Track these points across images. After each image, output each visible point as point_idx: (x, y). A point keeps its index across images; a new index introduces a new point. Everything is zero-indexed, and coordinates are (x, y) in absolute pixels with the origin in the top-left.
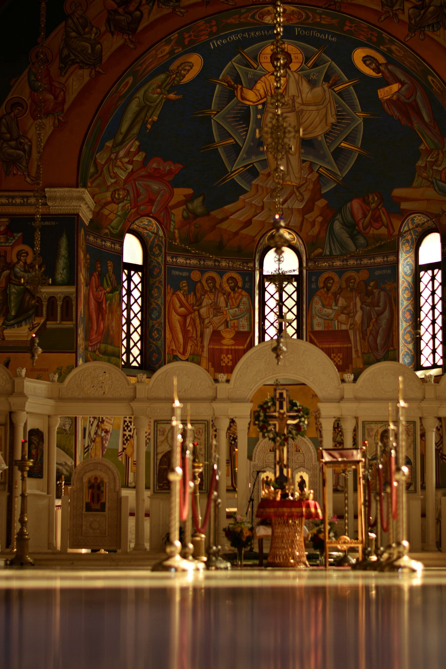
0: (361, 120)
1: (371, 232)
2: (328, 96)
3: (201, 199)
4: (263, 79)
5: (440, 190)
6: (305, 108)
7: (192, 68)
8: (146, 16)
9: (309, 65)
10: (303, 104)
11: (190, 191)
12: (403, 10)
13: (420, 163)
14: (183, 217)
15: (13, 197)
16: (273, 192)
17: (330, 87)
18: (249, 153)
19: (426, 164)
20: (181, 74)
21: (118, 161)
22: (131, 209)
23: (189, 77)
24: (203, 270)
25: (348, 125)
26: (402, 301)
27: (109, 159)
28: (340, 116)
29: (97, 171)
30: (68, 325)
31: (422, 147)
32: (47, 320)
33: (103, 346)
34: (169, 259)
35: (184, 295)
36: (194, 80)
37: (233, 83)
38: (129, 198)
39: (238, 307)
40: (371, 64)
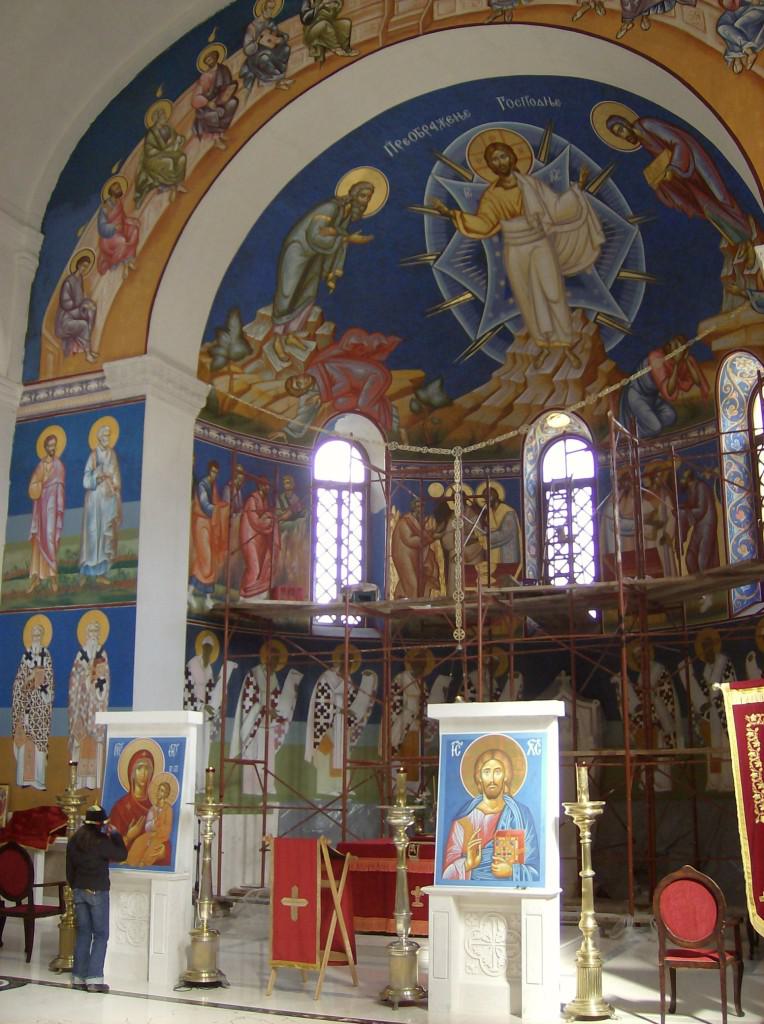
0: (636, 230)
1: (680, 397)
2: (583, 204)
4: (487, 195)
5: (759, 306)
6: (558, 229)
7: (373, 192)
8: (241, 103)
9: (542, 158)
13: (726, 272)
14: (412, 410)
15: (70, 386)
16: (536, 361)
17: (583, 188)
18: (497, 310)
19: (734, 271)
20: (358, 202)
21: (291, 336)
22: (322, 402)
23: (376, 203)
26: (730, 493)
28: (608, 230)
31: (723, 245)
37: (446, 209)
38: (316, 387)
40: (620, 130)
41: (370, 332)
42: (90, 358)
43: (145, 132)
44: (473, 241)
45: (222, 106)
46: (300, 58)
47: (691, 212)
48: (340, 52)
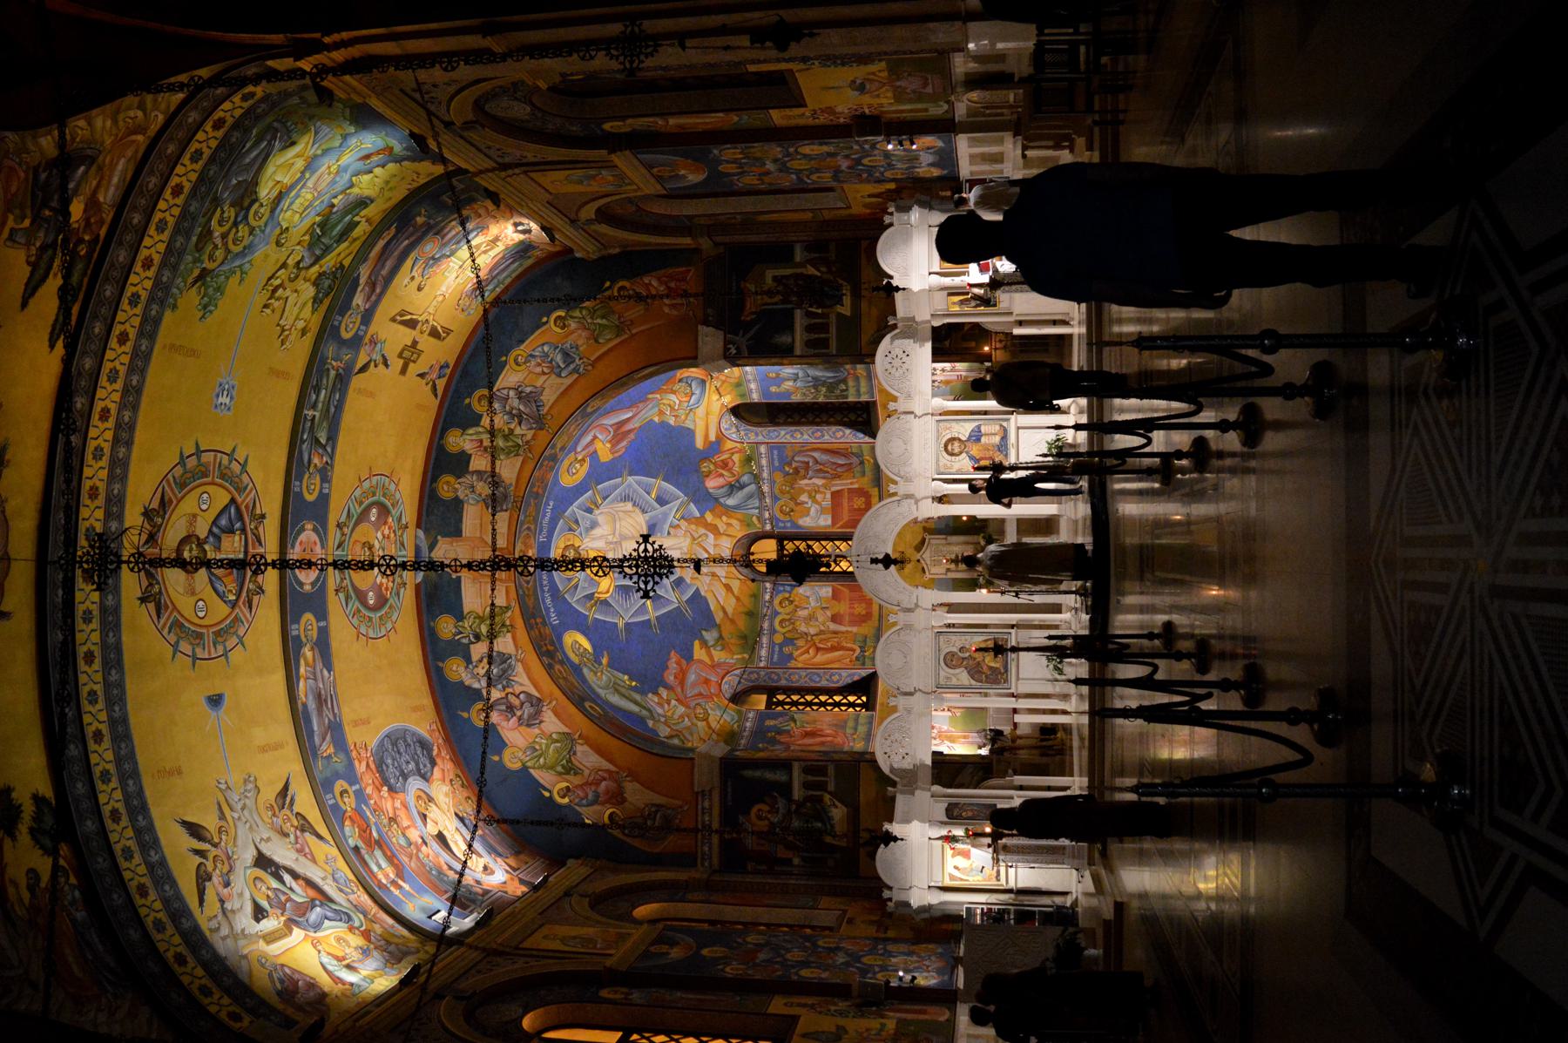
0: (630, 479)
3: (704, 633)
6: (617, 532)
10: (614, 534)
11: (697, 643)
12: (523, 435)
13: (672, 421)
23: (586, 644)
24: (773, 631)
25: (634, 491)
27: (665, 723)
28: (626, 498)
29: (677, 736)
30: (831, 770)
31: (656, 419)
32: (826, 791)
33: (849, 731)
34: (762, 665)
35: (797, 650)
36: (590, 640)
39: (808, 597)
41: (667, 667)
42: (685, 808)
43: (525, 769)
44: (615, 590)
45: (522, 704)
46: (504, 644)
47: (632, 436)
48: (509, 614)
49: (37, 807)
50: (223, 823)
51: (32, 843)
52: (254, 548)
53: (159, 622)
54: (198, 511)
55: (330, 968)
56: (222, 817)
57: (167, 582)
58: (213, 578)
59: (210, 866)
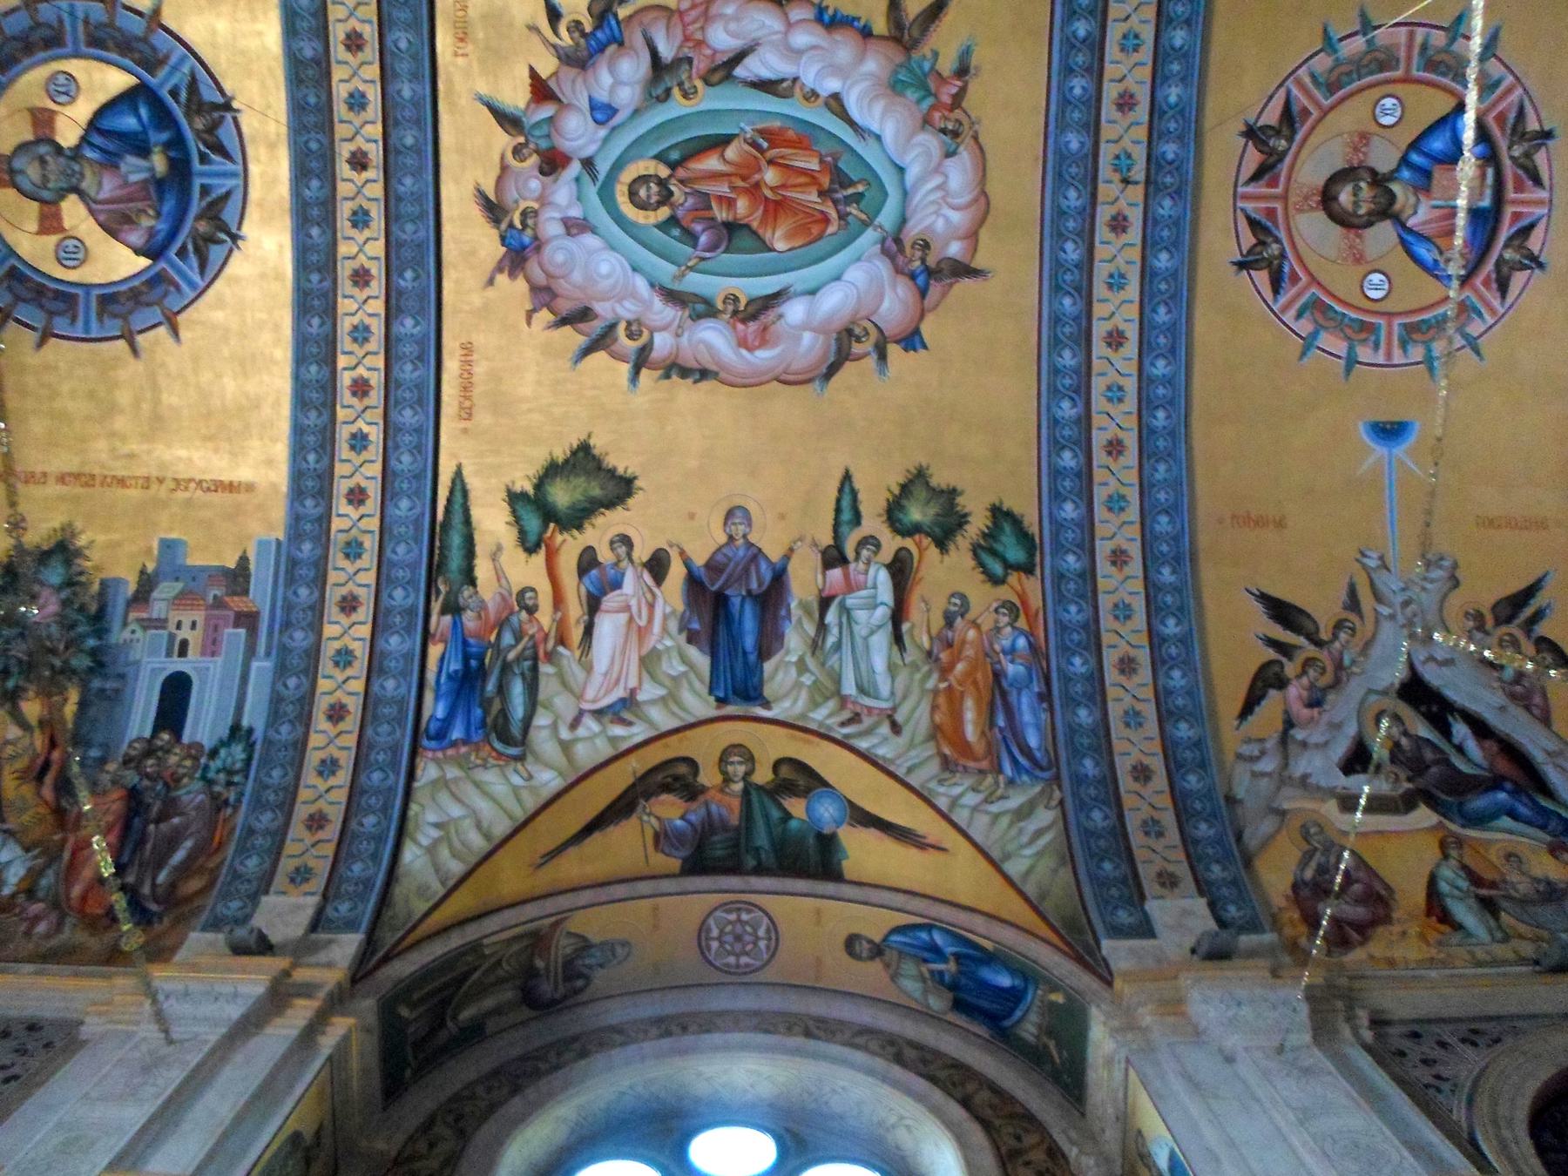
49: (995, 523)
50: (1353, 617)
51: (973, 563)
52: (1519, 188)
53: (1275, 300)
54: (1374, 128)
55: (1444, 887)
56: (1353, 603)
57: (1297, 239)
58: (1410, 238)
59: (1290, 669)
